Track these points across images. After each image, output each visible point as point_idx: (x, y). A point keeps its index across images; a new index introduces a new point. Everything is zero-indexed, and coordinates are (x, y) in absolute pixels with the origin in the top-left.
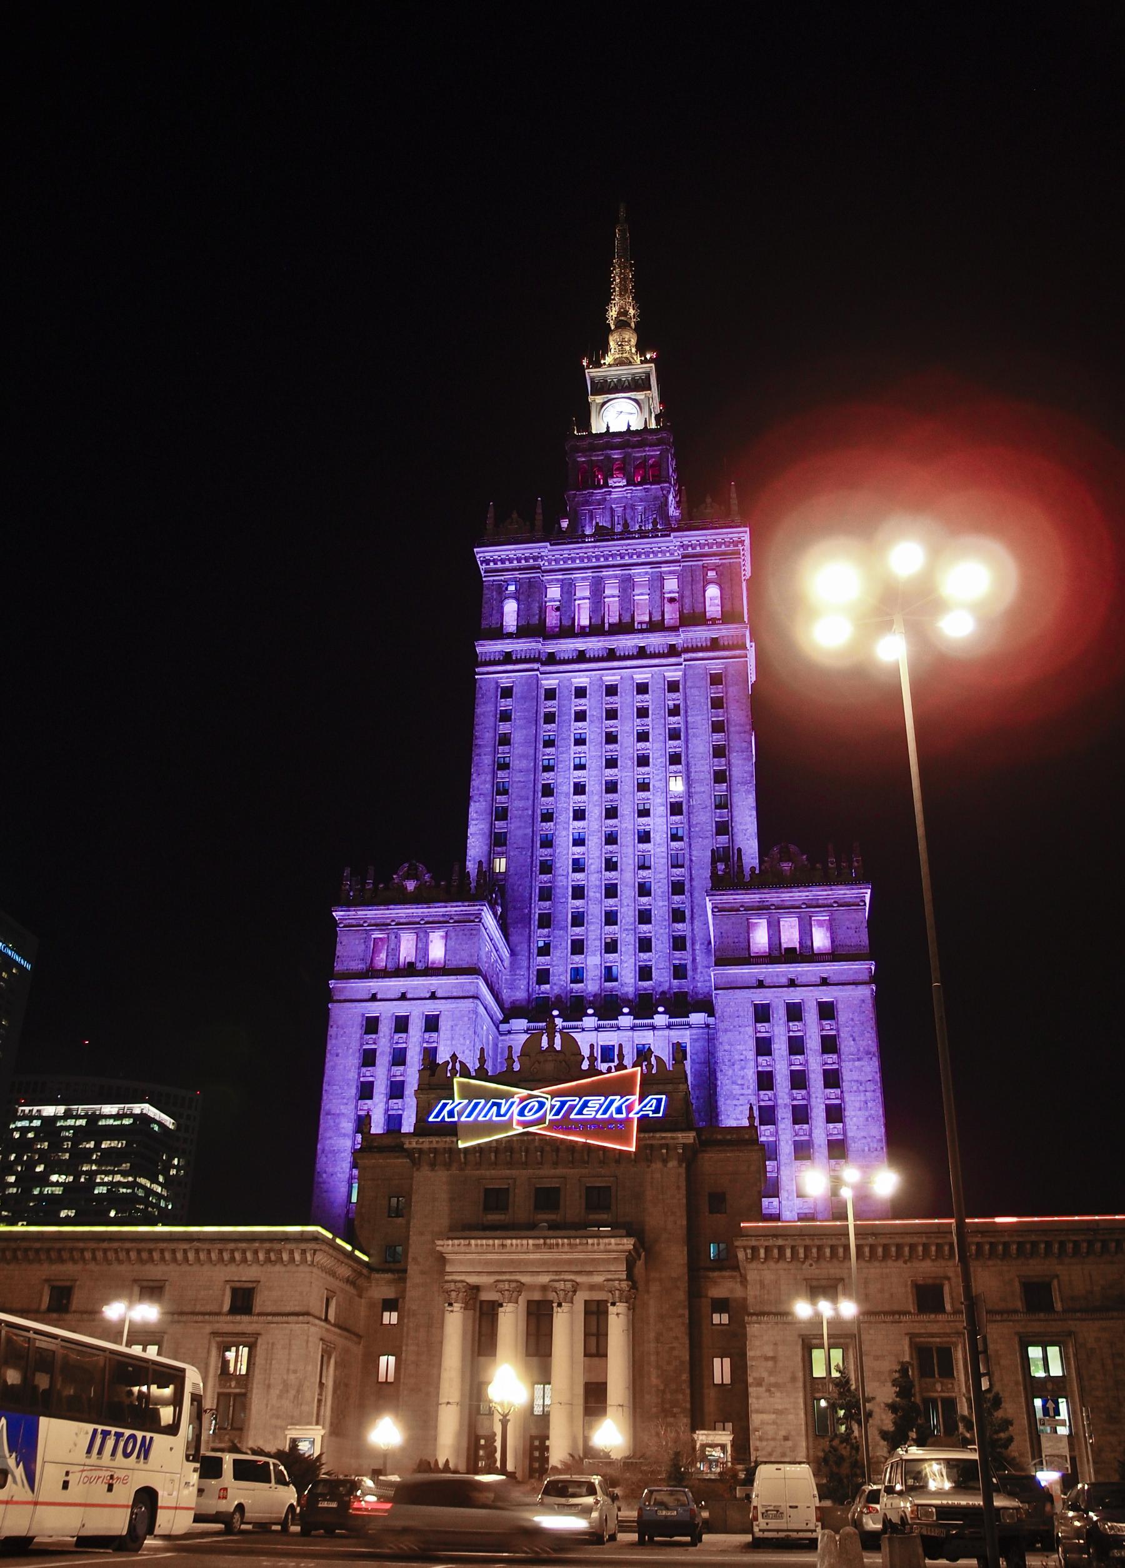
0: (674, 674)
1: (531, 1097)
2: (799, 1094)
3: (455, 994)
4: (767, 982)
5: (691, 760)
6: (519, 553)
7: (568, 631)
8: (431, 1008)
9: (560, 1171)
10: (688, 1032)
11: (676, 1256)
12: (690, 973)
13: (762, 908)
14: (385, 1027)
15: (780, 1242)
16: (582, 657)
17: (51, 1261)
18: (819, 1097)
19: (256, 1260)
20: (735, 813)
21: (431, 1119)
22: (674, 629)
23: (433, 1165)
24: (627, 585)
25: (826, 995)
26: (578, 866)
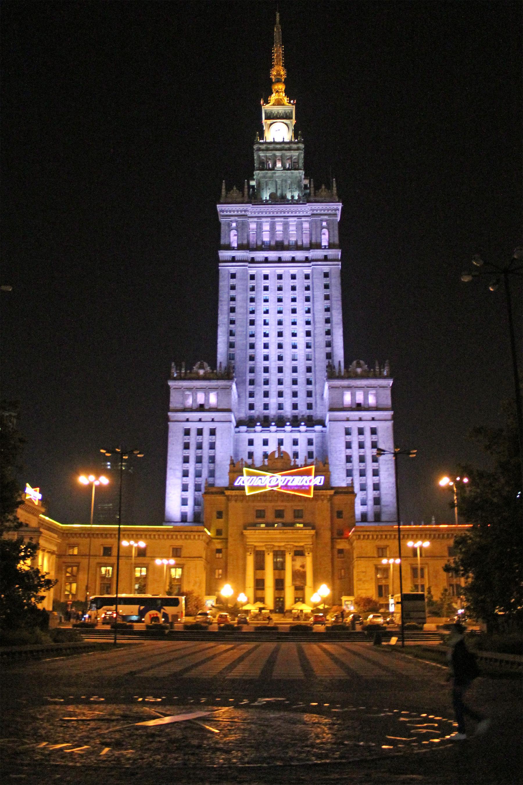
0: (308, 271)
1: (273, 476)
2: (362, 464)
3: (222, 420)
4: (351, 418)
5: (315, 313)
6: (238, 208)
8: (212, 425)
9: (284, 504)
10: (314, 434)
11: (327, 535)
12: (314, 407)
13: (349, 388)
14: (193, 433)
16: (266, 260)
19: (181, 538)
20: (334, 338)
22: (308, 249)
24: (286, 226)
25: (374, 424)
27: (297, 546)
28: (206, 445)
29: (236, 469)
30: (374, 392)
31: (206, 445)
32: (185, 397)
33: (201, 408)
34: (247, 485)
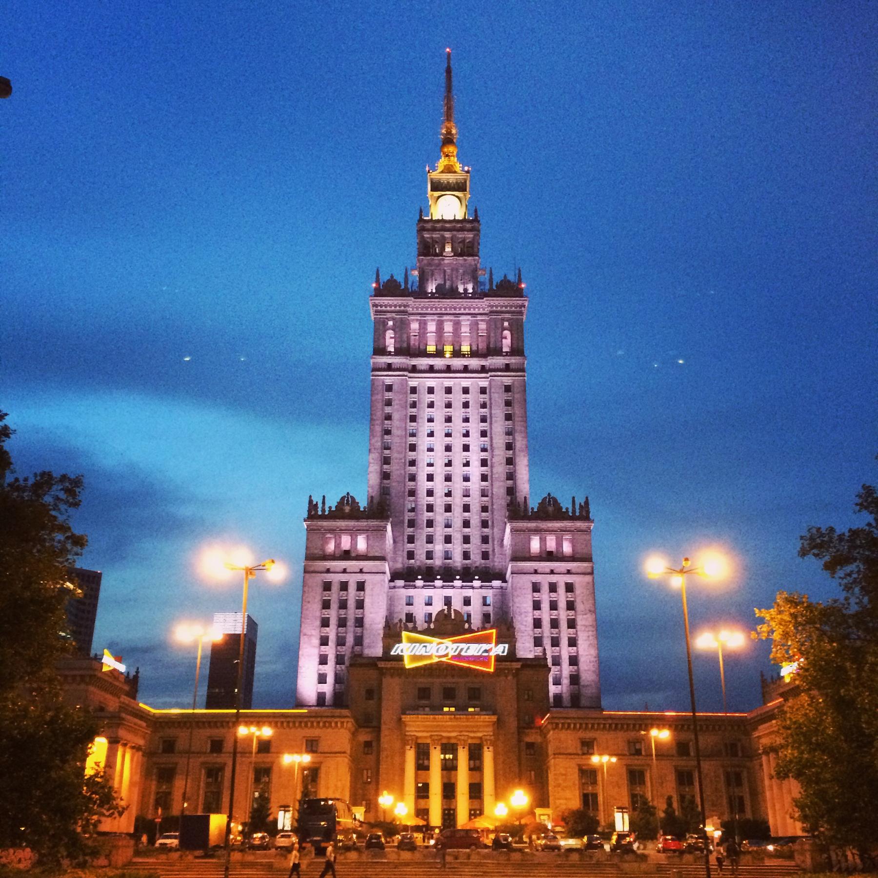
0: (484, 383)
2: (555, 631)
5: (493, 436)
7: (424, 354)
8: (360, 577)
9: (455, 680)
10: (491, 591)
11: (512, 723)
12: (491, 557)
13: (537, 531)
14: (335, 588)
15: (569, 721)
16: (431, 369)
17: (210, 727)
18: (565, 634)
21: (392, 653)
22: (484, 356)
23: (392, 676)
25: (569, 579)
26: (430, 493)
27: (472, 738)
28: (351, 604)
29: (392, 634)
32: (326, 541)
33: (346, 555)
34: (406, 655)
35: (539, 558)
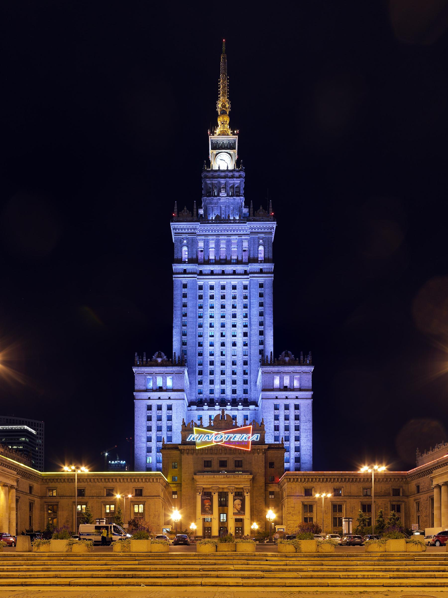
0: (246, 282)
1: (218, 434)
3: (177, 398)
7: (208, 262)
8: (169, 402)
9: (227, 456)
11: (261, 480)
13: (278, 373)
16: (212, 273)
22: (246, 264)
27: (237, 488)
28: (164, 418)
30: (298, 376)
31: (164, 418)
32: (148, 381)
33: (160, 389)
35: (280, 390)
